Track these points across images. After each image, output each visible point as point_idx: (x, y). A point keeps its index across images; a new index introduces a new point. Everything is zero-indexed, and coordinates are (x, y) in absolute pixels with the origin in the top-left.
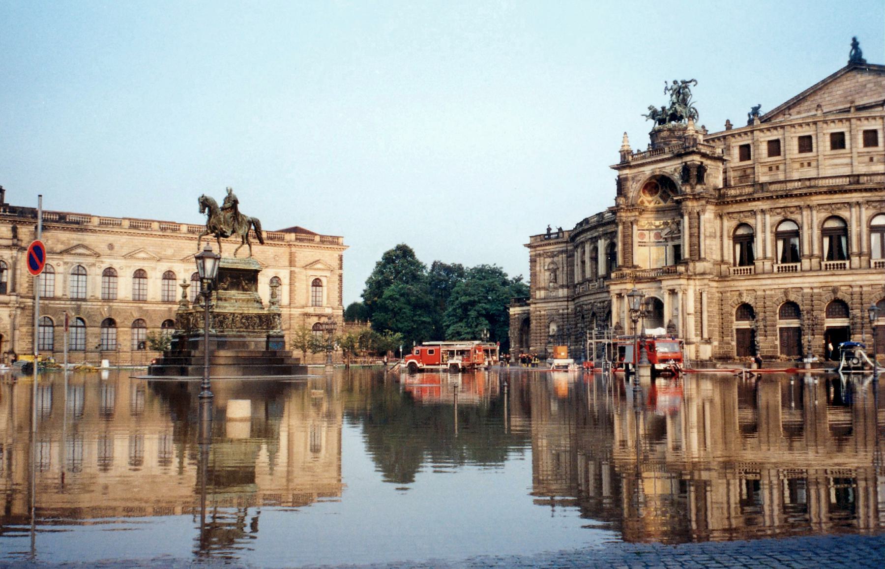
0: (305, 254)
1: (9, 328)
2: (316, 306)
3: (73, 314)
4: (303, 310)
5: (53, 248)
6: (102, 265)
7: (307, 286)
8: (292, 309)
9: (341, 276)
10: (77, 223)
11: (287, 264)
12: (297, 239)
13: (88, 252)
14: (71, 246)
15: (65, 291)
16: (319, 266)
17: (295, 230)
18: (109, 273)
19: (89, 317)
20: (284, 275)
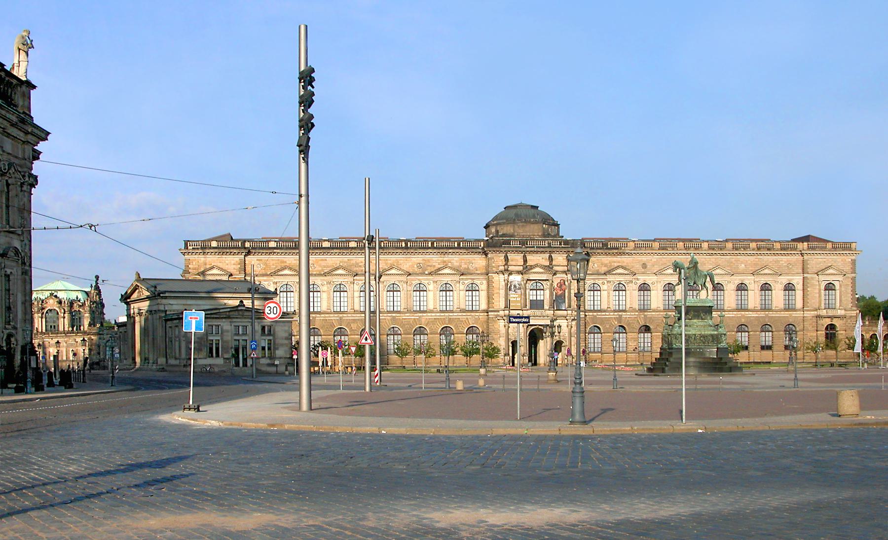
0: (817, 260)
1: (567, 335)
2: (829, 308)
3: (616, 323)
4: (816, 312)
5: (599, 270)
6: (637, 281)
7: (820, 290)
8: (805, 312)
9: (854, 279)
10: (617, 249)
11: (801, 271)
12: (809, 248)
13: (626, 272)
14: (612, 268)
15: (609, 305)
16: (831, 271)
17: (806, 239)
18: (644, 288)
19: (629, 325)
20: (797, 281)
